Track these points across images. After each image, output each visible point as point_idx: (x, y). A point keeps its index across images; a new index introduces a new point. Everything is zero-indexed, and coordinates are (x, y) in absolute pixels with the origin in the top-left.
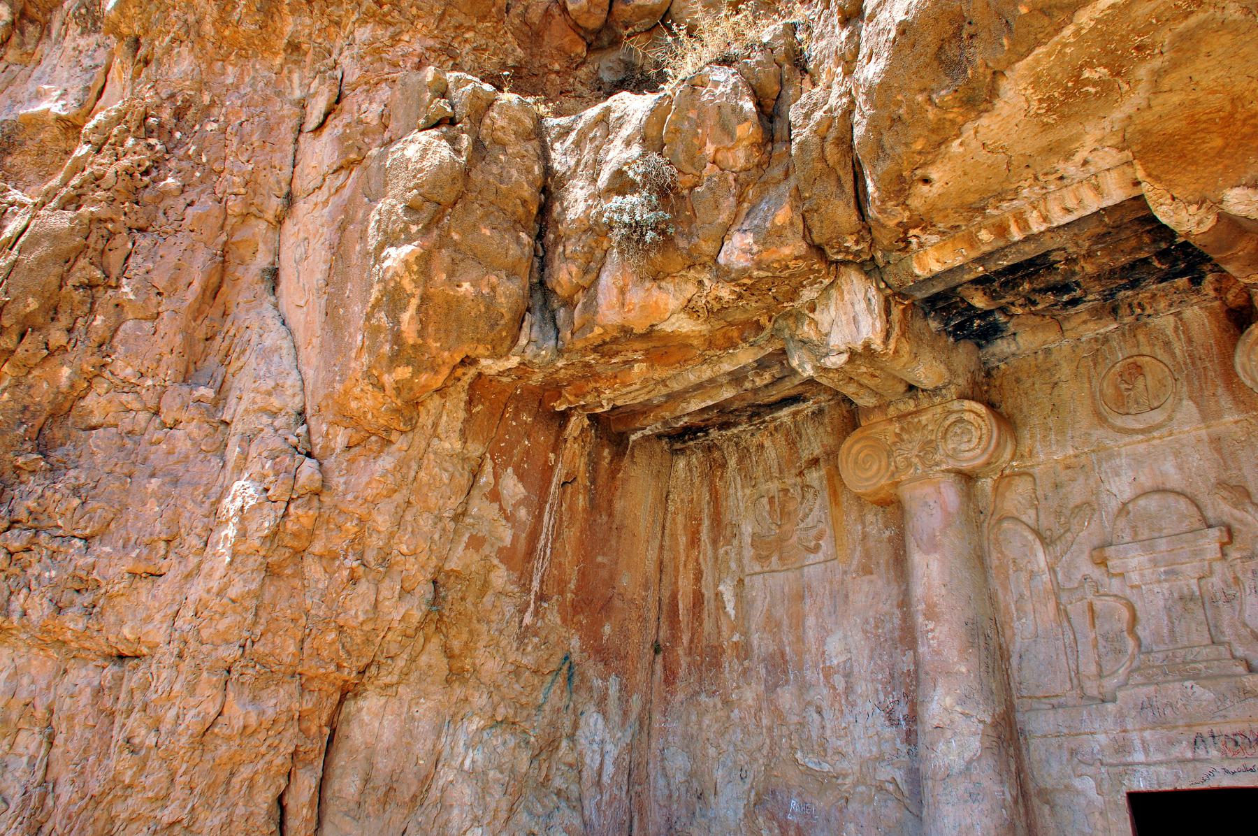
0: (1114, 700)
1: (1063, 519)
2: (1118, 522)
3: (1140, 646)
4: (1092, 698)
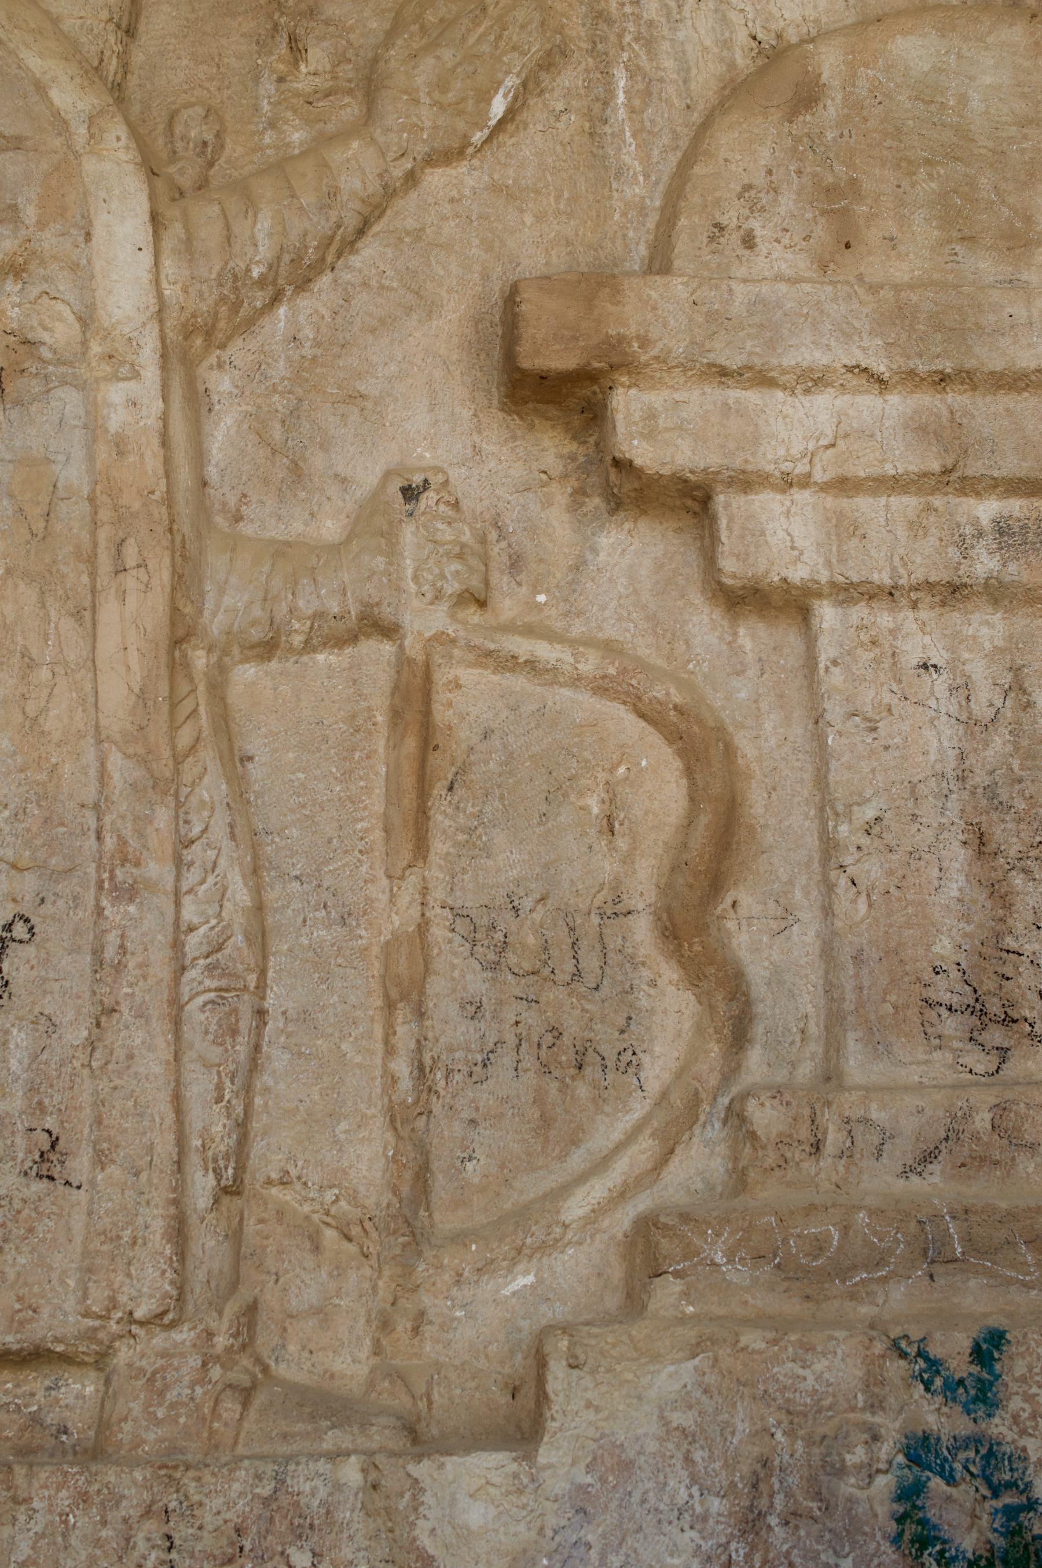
0: (520, 1423)
1: (317, 57)
2: (725, 140)
3: (739, 1036)
4: (326, 1406)
